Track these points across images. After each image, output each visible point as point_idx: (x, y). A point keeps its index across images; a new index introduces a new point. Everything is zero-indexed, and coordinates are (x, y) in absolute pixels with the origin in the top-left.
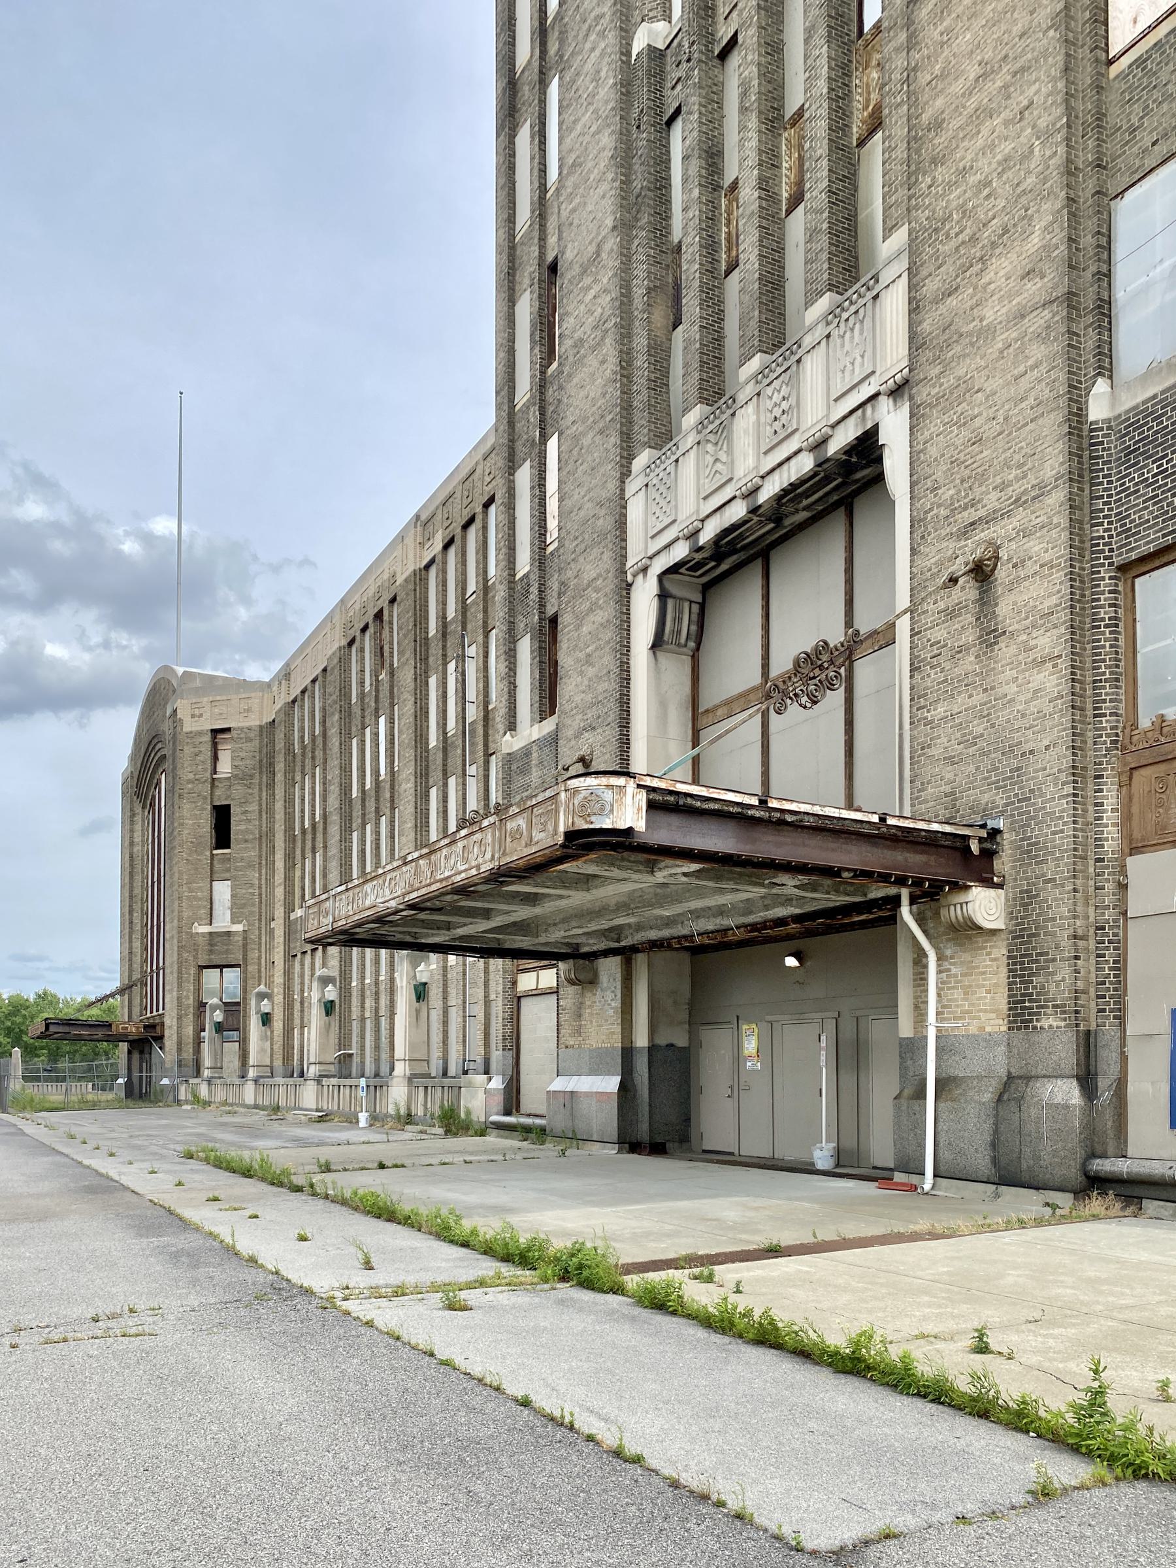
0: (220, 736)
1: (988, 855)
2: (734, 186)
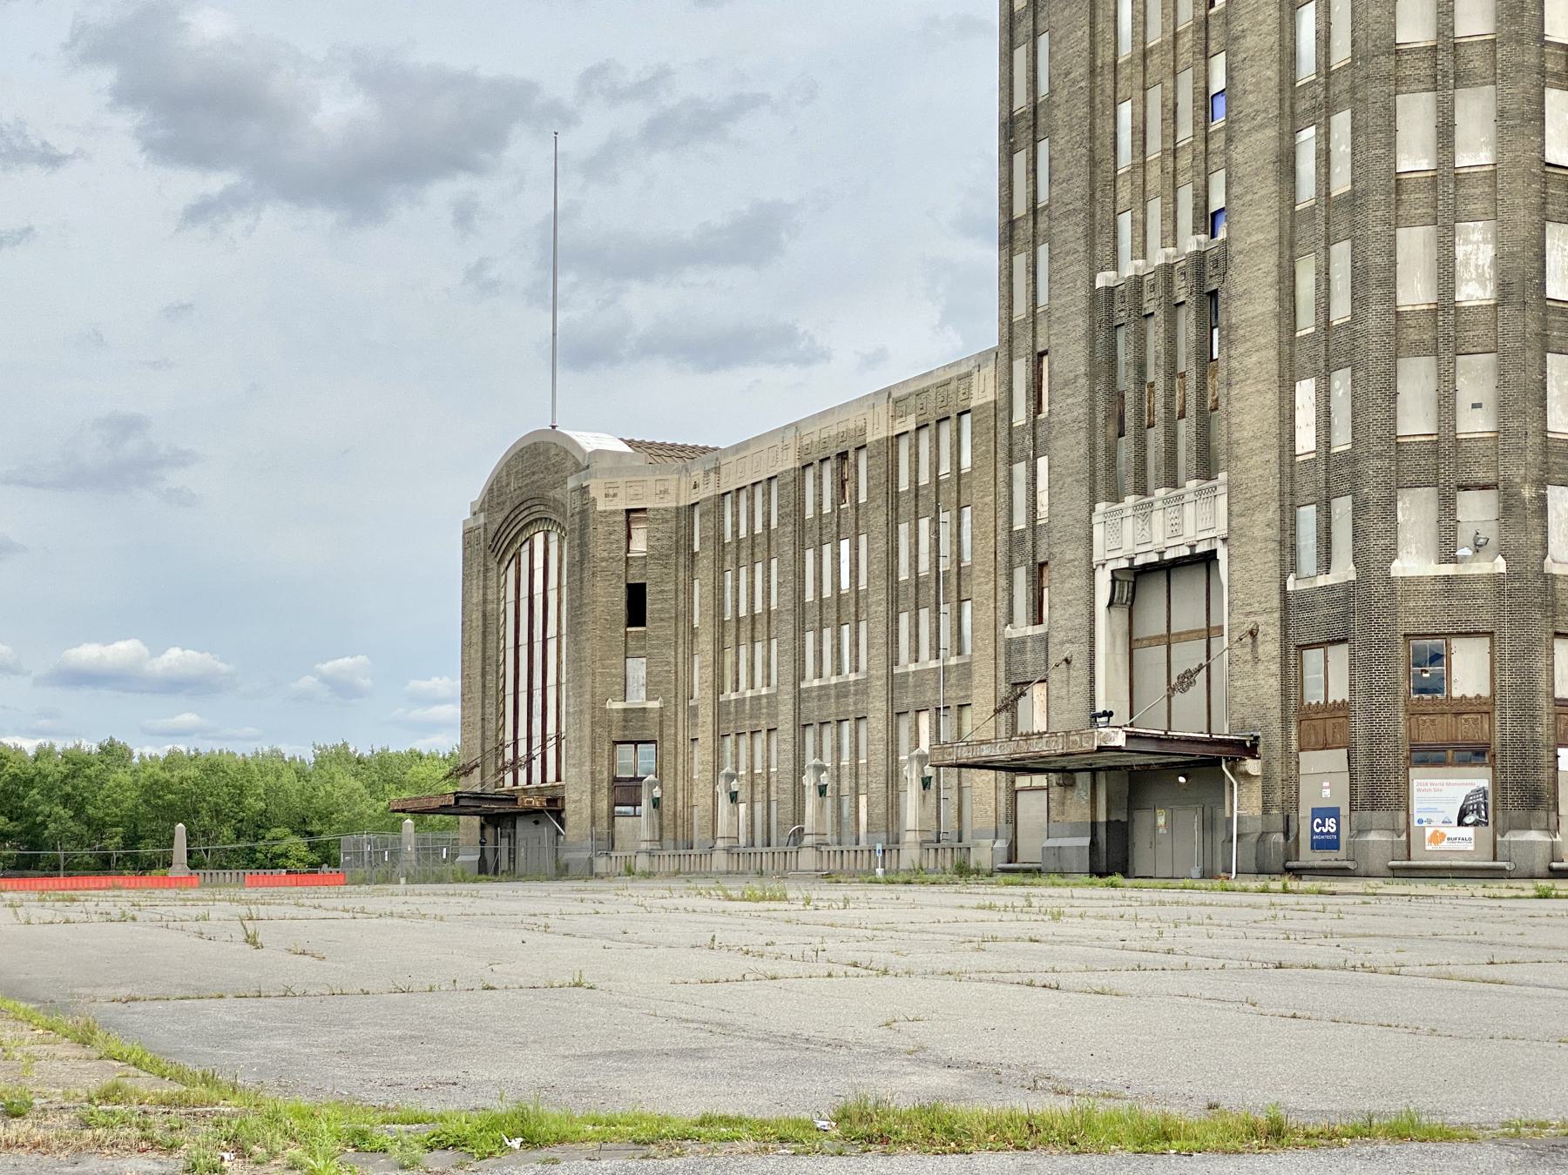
0: (633, 515)
1: (1254, 746)
2: (1152, 385)
